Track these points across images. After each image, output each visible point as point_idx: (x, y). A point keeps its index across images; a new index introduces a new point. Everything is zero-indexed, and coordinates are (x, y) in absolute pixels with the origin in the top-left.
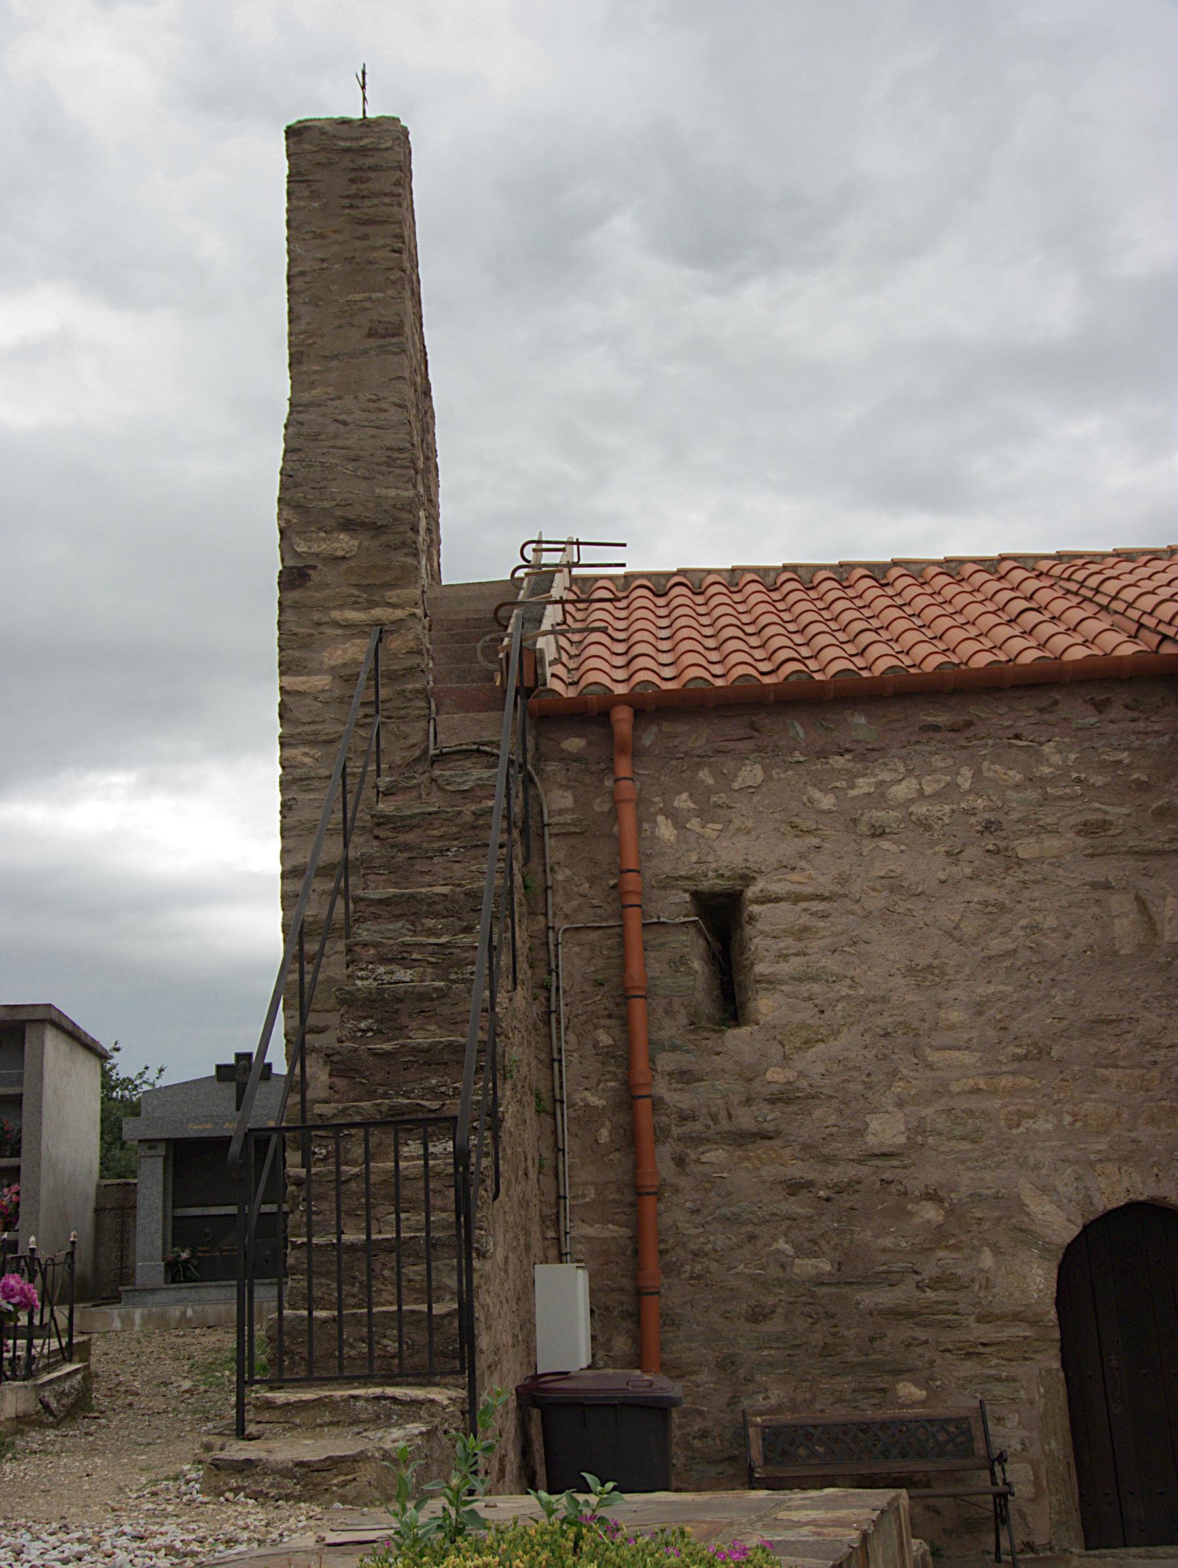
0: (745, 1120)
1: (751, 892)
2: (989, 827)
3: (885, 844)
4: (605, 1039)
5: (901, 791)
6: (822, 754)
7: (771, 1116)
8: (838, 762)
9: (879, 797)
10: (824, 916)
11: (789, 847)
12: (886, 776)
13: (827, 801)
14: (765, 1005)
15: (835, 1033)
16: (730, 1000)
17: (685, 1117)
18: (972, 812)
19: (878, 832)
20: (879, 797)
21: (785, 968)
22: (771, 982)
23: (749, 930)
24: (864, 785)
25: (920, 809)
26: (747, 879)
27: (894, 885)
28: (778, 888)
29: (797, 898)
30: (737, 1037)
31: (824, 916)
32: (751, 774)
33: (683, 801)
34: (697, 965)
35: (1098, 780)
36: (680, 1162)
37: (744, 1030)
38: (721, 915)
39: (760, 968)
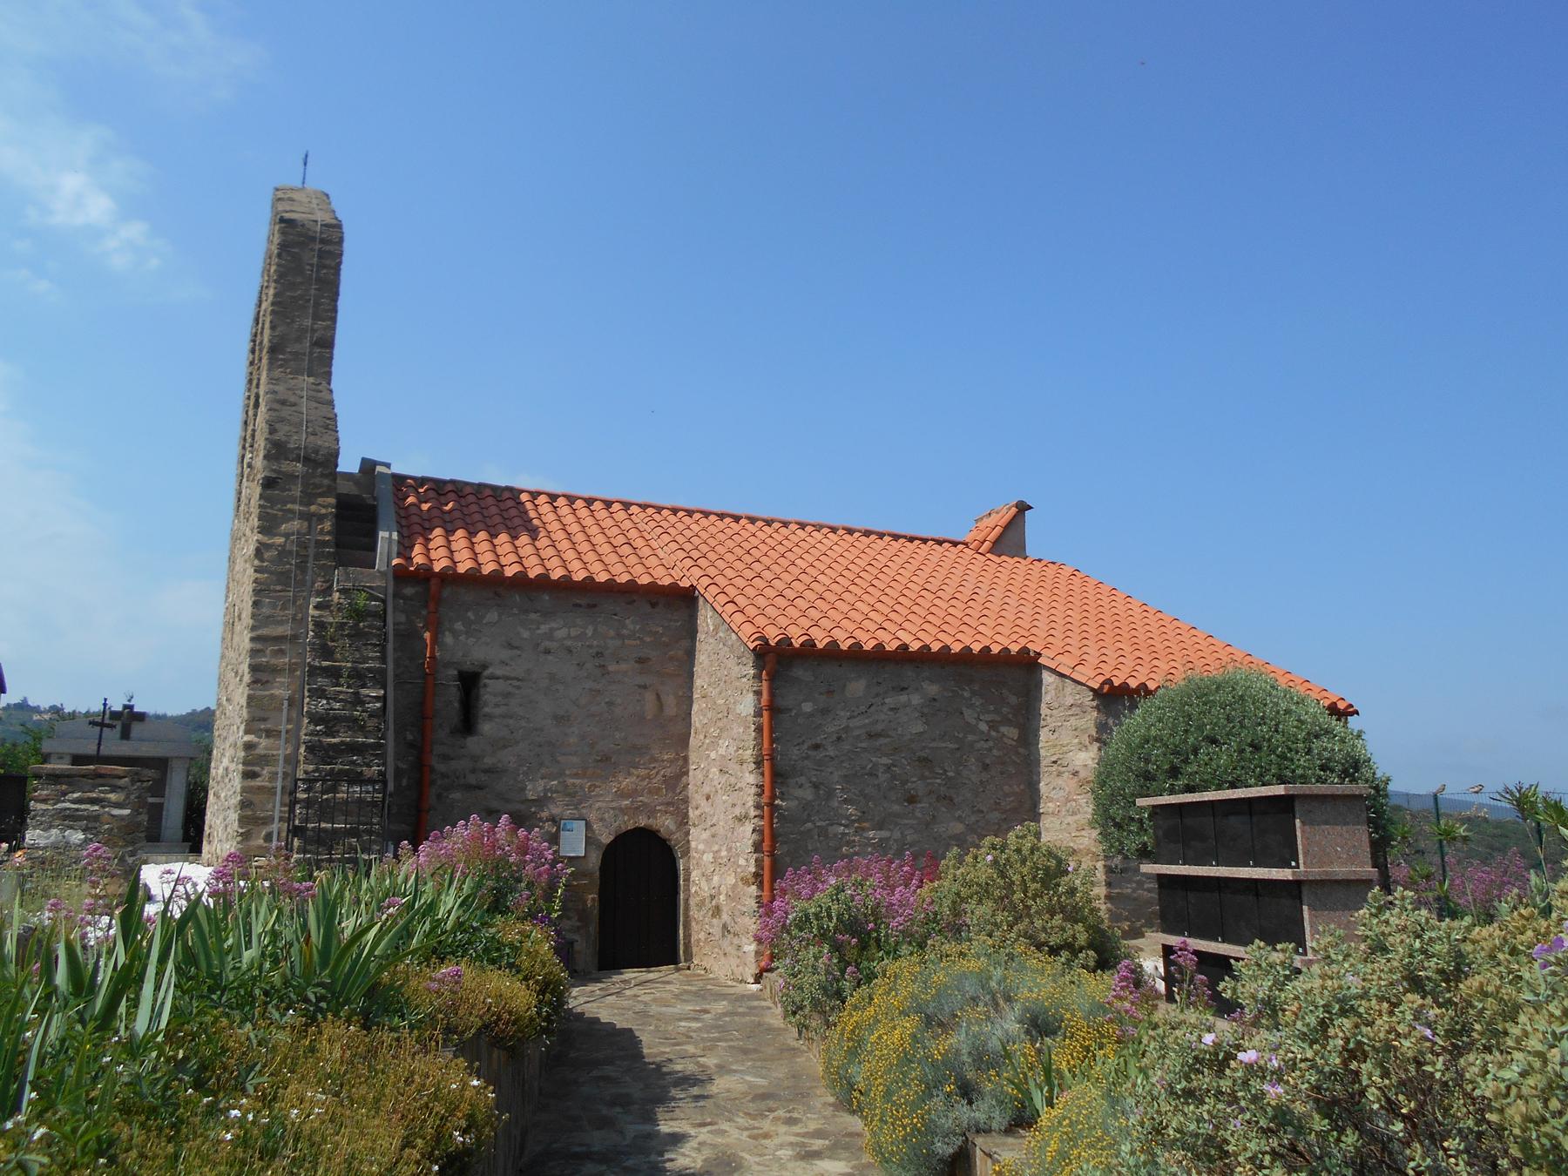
0: (472, 780)
1: (486, 673)
2: (599, 654)
3: (550, 657)
4: (410, 737)
5: (561, 633)
6: (526, 612)
7: (484, 777)
8: (533, 616)
9: (549, 636)
10: (519, 688)
11: (505, 654)
12: (554, 625)
13: (526, 634)
14: (486, 728)
15: (517, 743)
16: (468, 723)
17: (444, 776)
18: (590, 647)
19: (547, 652)
20: (549, 636)
21: (497, 711)
22: (489, 717)
23: (482, 691)
24: (544, 628)
25: (568, 643)
26: (485, 667)
27: (552, 677)
28: (499, 672)
29: (507, 678)
30: (472, 743)
31: (519, 688)
32: (492, 616)
33: (459, 626)
34: (456, 705)
35: (648, 639)
36: (439, 796)
37: (475, 739)
38: (470, 681)
39: (486, 710)
